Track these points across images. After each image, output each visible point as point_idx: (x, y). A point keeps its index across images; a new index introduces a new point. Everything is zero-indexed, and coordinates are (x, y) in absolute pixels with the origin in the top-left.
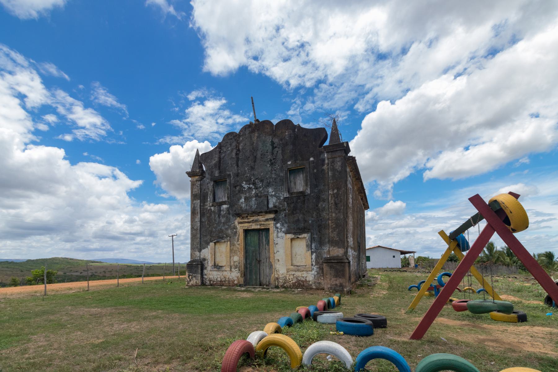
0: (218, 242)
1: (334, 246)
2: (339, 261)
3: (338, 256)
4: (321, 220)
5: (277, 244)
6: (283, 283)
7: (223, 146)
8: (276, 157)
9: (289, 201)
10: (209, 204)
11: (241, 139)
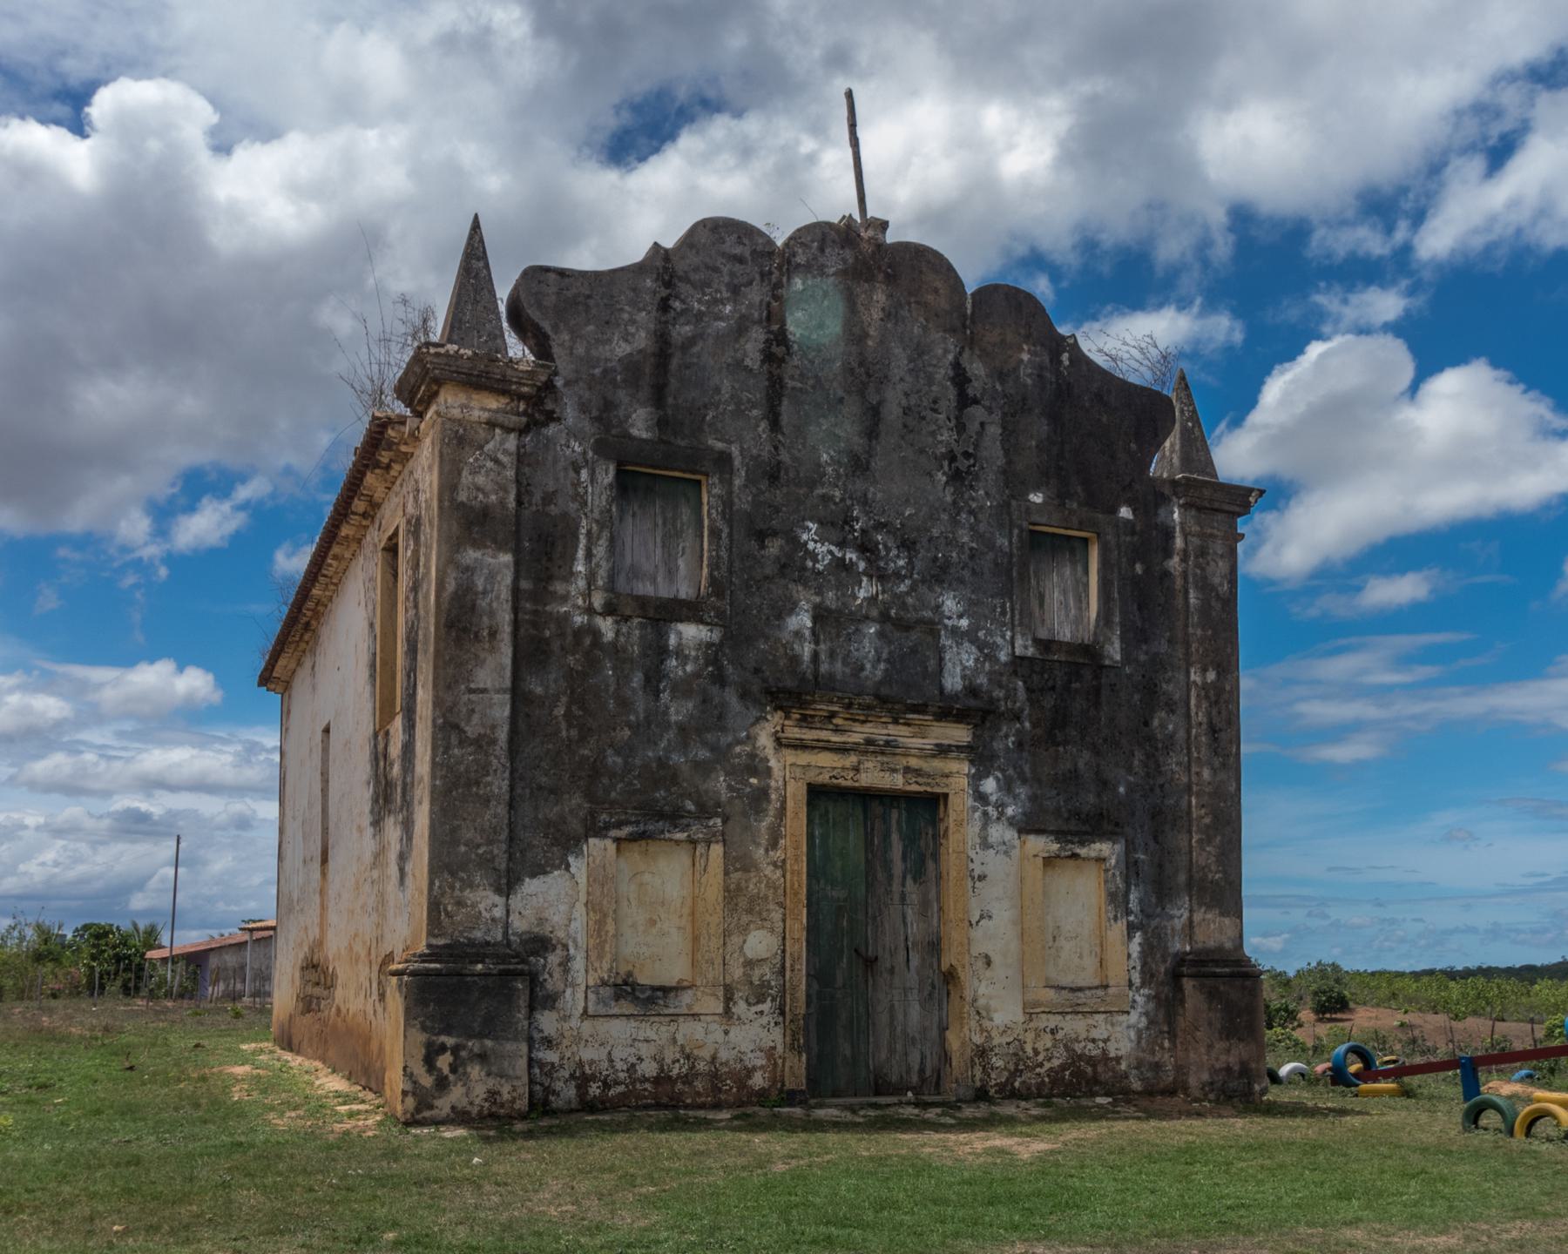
0: (634, 838)
1: (1209, 907)
2: (1236, 969)
3: (1220, 949)
4: (1162, 786)
5: (982, 878)
6: (1006, 1074)
7: (688, 281)
8: (976, 446)
9: (1035, 677)
10: (587, 595)
11: (798, 283)
